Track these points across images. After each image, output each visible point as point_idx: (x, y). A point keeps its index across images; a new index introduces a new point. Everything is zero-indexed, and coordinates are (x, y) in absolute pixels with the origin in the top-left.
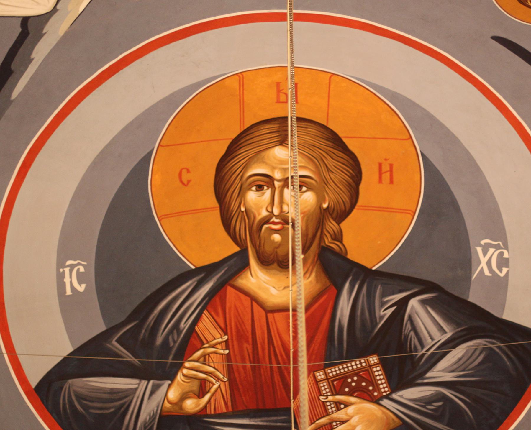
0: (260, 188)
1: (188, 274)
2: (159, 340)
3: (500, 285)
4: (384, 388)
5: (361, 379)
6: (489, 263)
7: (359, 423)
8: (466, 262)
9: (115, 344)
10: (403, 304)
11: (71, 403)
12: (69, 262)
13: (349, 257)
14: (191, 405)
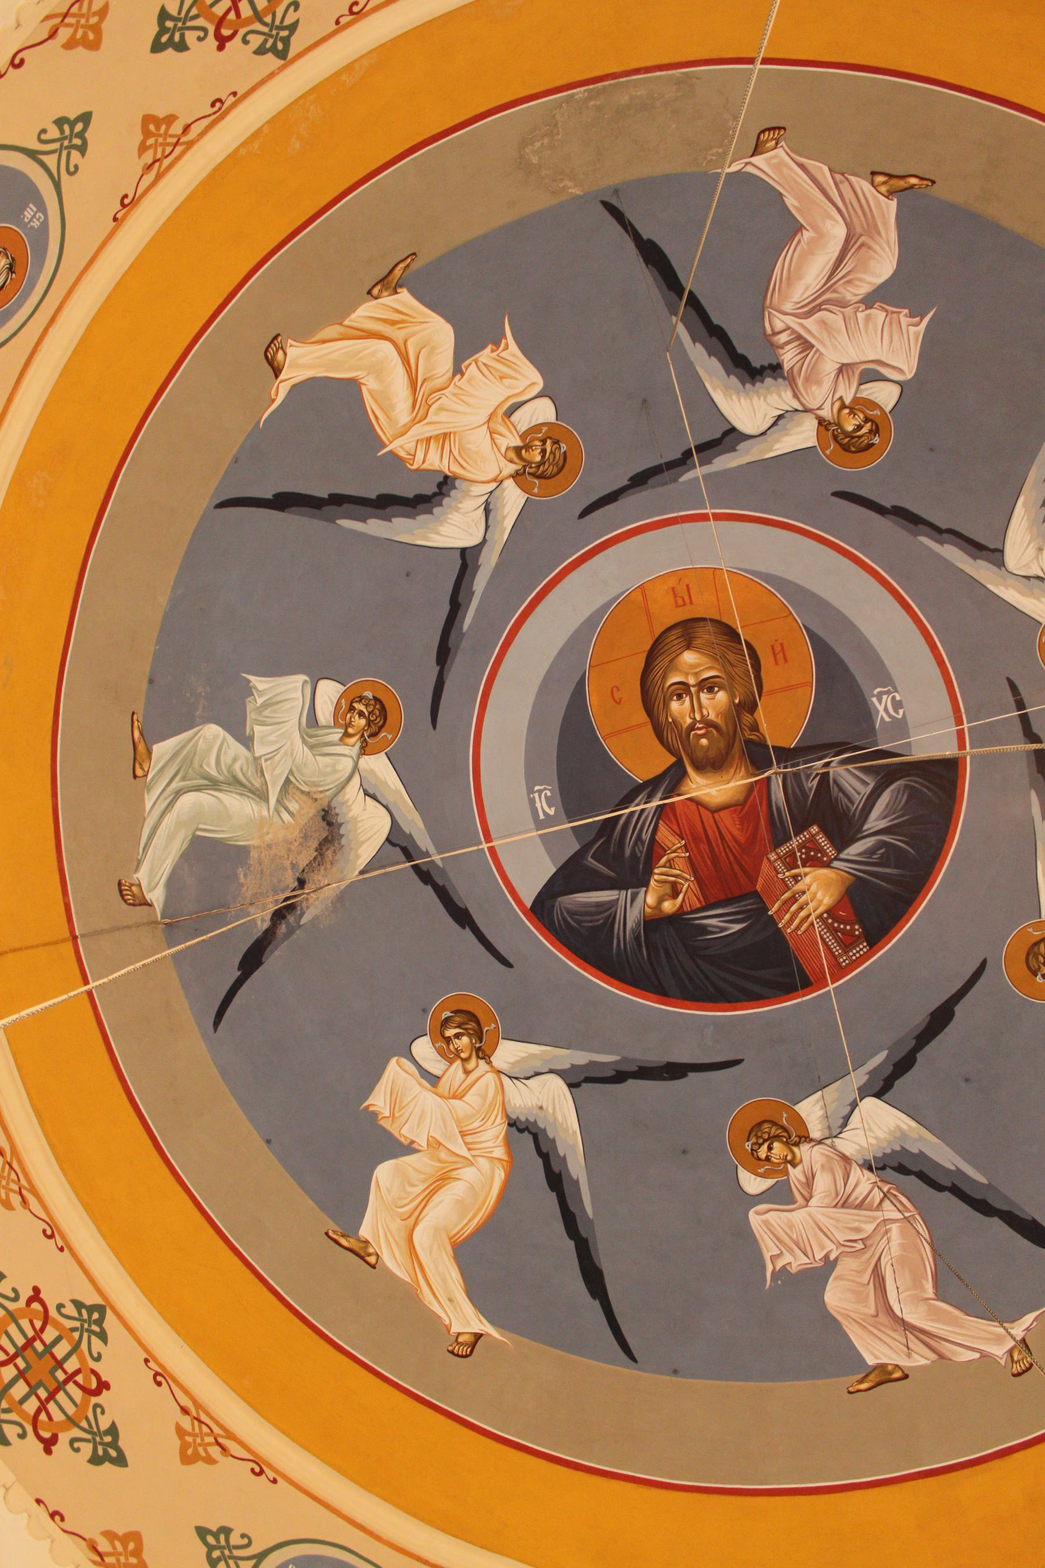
0: (680, 697)
2: (628, 852)
3: (900, 727)
4: (831, 851)
5: (809, 850)
6: (886, 710)
7: (818, 889)
8: (867, 714)
9: (590, 861)
11: (564, 919)
12: (537, 788)
14: (669, 907)
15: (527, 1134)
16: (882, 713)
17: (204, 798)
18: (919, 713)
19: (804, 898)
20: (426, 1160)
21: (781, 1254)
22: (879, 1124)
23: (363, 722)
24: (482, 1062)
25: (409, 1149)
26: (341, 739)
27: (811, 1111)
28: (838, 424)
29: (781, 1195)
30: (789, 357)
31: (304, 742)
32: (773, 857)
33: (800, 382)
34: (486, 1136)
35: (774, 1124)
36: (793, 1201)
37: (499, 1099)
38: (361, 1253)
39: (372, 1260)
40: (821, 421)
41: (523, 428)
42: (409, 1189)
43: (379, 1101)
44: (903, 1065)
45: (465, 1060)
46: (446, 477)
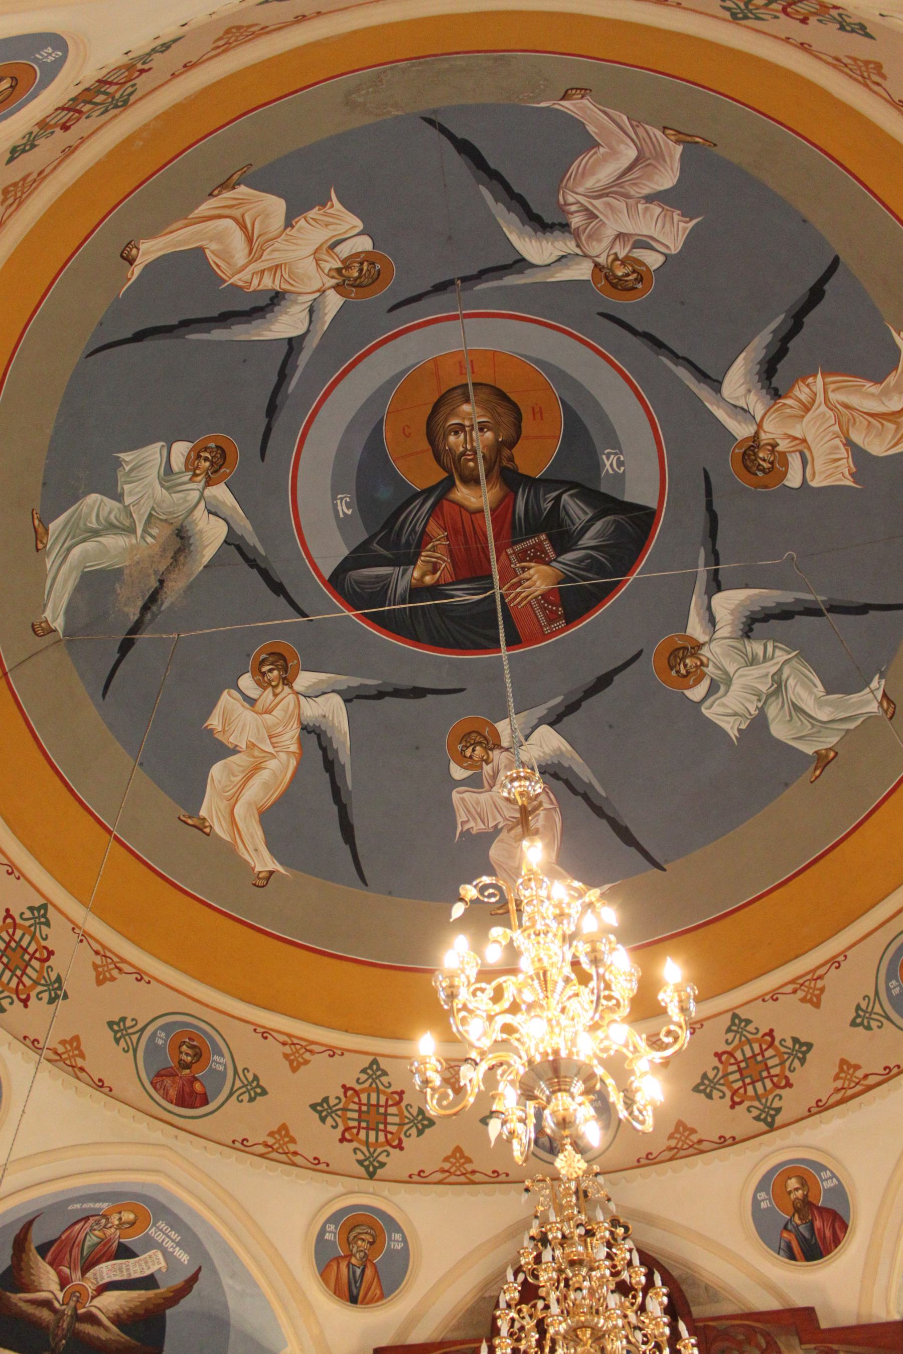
0: (456, 433)
1: (417, 495)
2: (403, 540)
3: (619, 478)
4: (552, 555)
6: (611, 465)
7: (538, 579)
8: (597, 466)
9: (375, 546)
10: (558, 498)
11: (353, 588)
12: (339, 496)
13: (520, 471)
14: (428, 579)
15: (314, 734)
16: (608, 466)
18: (634, 469)
19: (527, 584)
20: (244, 757)
21: (468, 821)
23: (208, 464)
24: (286, 688)
26: (191, 479)
28: (611, 270)
29: (475, 783)
30: (576, 221)
31: (162, 486)
32: (509, 551)
33: (583, 238)
35: (479, 733)
36: (482, 787)
37: (296, 712)
38: (201, 827)
39: (207, 830)
40: (597, 265)
41: (344, 255)
42: (233, 779)
43: (215, 721)
44: (571, 708)
45: (274, 687)
46: (277, 293)
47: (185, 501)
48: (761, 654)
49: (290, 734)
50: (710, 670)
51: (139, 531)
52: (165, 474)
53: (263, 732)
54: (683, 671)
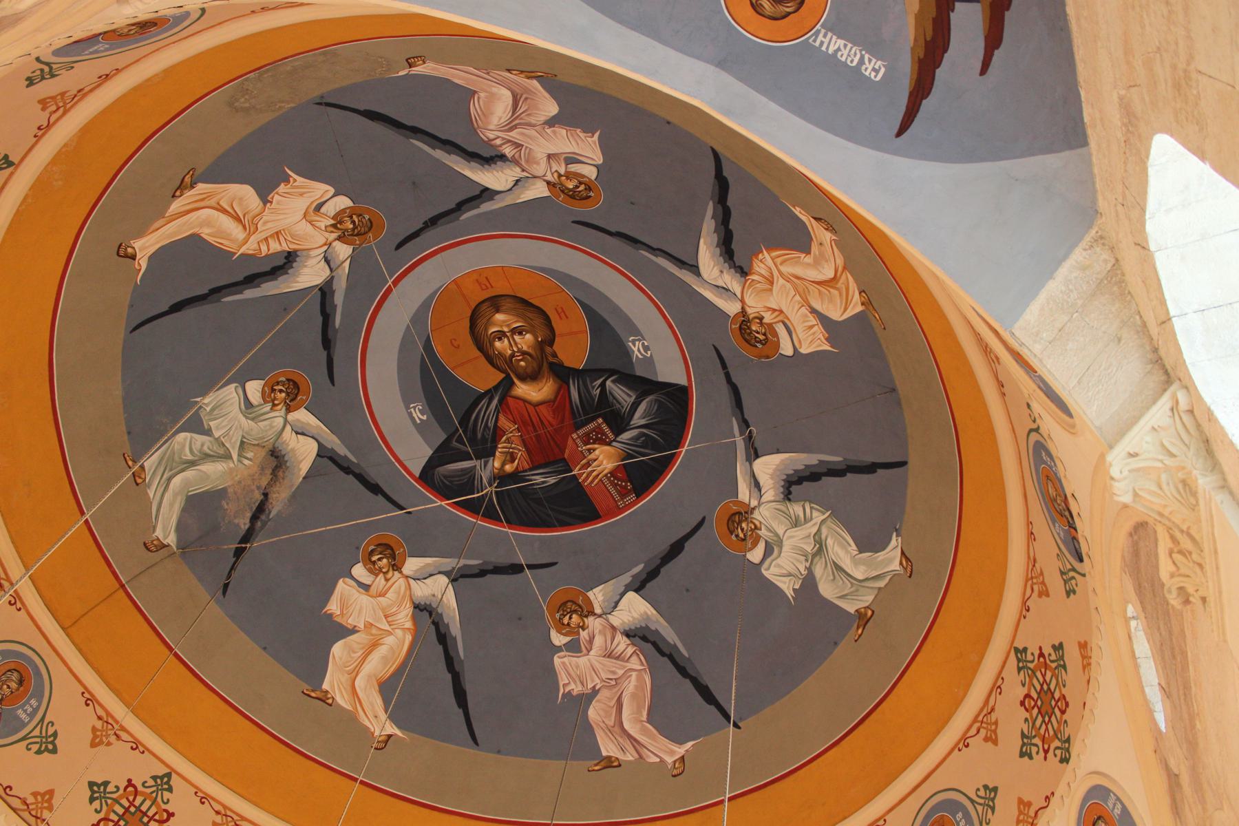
0: (500, 339)
1: (481, 397)
2: (479, 436)
3: (650, 362)
5: (597, 433)
8: (627, 353)
9: (455, 444)
10: (603, 385)
14: (509, 468)
15: (425, 611)
17: (189, 474)
22: (635, 608)
23: (283, 395)
25: (354, 631)
27: (597, 596)
29: (574, 647)
31: (247, 418)
32: (575, 436)
34: (400, 616)
35: (574, 603)
36: (580, 651)
38: (324, 699)
39: (330, 701)
43: (333, 607)
44: (652, 574)
47: (272, 427)
48: (802, 515)
49: (405, 612)
50: (763, 532)
51: (235, 456)
52: (247, 408)
53: (378, 614)
54: (741, 535)
